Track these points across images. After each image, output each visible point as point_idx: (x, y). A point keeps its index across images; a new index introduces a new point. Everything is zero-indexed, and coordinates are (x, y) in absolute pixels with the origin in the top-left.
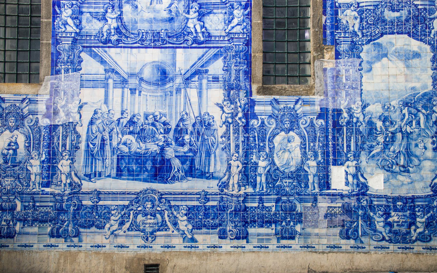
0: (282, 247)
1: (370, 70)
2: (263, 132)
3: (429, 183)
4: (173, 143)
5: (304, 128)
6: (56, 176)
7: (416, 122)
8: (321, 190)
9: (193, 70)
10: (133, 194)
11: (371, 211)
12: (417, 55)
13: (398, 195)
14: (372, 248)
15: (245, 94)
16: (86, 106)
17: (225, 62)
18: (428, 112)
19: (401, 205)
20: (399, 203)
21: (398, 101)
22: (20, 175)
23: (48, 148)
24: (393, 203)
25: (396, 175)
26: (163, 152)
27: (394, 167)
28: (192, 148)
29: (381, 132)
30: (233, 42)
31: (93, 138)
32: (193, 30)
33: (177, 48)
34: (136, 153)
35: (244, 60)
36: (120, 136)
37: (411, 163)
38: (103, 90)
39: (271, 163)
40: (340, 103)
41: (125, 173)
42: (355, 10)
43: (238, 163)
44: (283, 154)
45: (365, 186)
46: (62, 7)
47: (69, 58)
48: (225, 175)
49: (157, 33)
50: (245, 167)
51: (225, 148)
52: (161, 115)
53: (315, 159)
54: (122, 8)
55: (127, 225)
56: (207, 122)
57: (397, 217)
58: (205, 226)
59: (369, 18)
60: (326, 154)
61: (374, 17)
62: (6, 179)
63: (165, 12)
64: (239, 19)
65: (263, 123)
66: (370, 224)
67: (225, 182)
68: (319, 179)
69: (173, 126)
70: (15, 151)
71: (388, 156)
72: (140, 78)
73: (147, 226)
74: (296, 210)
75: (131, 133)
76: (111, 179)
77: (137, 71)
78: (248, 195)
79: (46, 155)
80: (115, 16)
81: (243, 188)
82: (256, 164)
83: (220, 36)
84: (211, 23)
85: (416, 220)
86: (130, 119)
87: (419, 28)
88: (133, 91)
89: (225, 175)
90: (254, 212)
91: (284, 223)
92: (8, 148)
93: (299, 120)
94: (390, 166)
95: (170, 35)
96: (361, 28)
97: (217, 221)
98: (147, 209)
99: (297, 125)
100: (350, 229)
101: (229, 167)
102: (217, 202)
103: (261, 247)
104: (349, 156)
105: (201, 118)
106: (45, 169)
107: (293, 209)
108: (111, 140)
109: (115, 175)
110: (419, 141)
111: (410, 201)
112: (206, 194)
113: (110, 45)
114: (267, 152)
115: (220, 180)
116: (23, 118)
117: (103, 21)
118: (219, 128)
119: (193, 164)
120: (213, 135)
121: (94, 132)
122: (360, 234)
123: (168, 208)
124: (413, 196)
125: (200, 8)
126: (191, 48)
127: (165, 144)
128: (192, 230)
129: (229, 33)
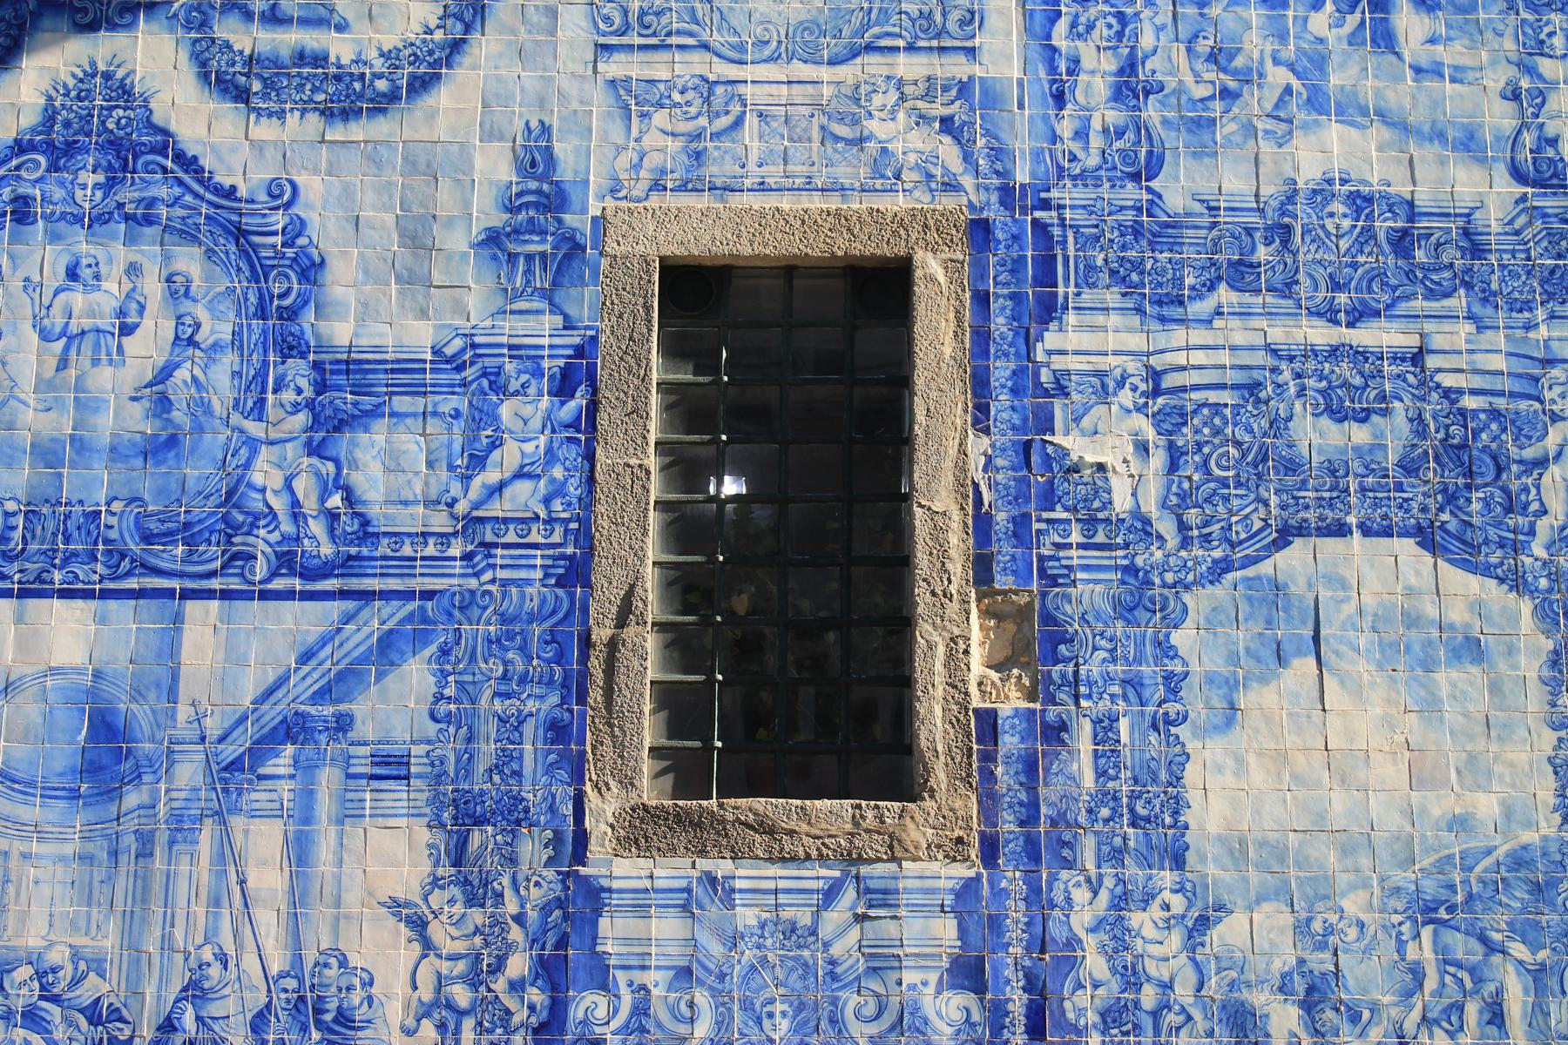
7: (1481, 1012)
9: (273, 713)
15: (550, 851)
18: (1542, 955)
30: (493, 566)
32: (279, 504)
33: (187, 595)
35: (549, 661)
40: (1068, 900)
49: (86, 515)
52: (82, 966)
56: (332, 1005)
59: (1216, 447)
61: (1238, 444)
63: (137, 409)
64: (529, 448)
65: (641, 1009)
83: (424, 534)
87: (1476, 506)
95: (154, 526)
96: (1174, 500)
99: (833, 1021)
105: (301, 981)
125: (321, 387)
126: (265, 595)
129: (473, 522)
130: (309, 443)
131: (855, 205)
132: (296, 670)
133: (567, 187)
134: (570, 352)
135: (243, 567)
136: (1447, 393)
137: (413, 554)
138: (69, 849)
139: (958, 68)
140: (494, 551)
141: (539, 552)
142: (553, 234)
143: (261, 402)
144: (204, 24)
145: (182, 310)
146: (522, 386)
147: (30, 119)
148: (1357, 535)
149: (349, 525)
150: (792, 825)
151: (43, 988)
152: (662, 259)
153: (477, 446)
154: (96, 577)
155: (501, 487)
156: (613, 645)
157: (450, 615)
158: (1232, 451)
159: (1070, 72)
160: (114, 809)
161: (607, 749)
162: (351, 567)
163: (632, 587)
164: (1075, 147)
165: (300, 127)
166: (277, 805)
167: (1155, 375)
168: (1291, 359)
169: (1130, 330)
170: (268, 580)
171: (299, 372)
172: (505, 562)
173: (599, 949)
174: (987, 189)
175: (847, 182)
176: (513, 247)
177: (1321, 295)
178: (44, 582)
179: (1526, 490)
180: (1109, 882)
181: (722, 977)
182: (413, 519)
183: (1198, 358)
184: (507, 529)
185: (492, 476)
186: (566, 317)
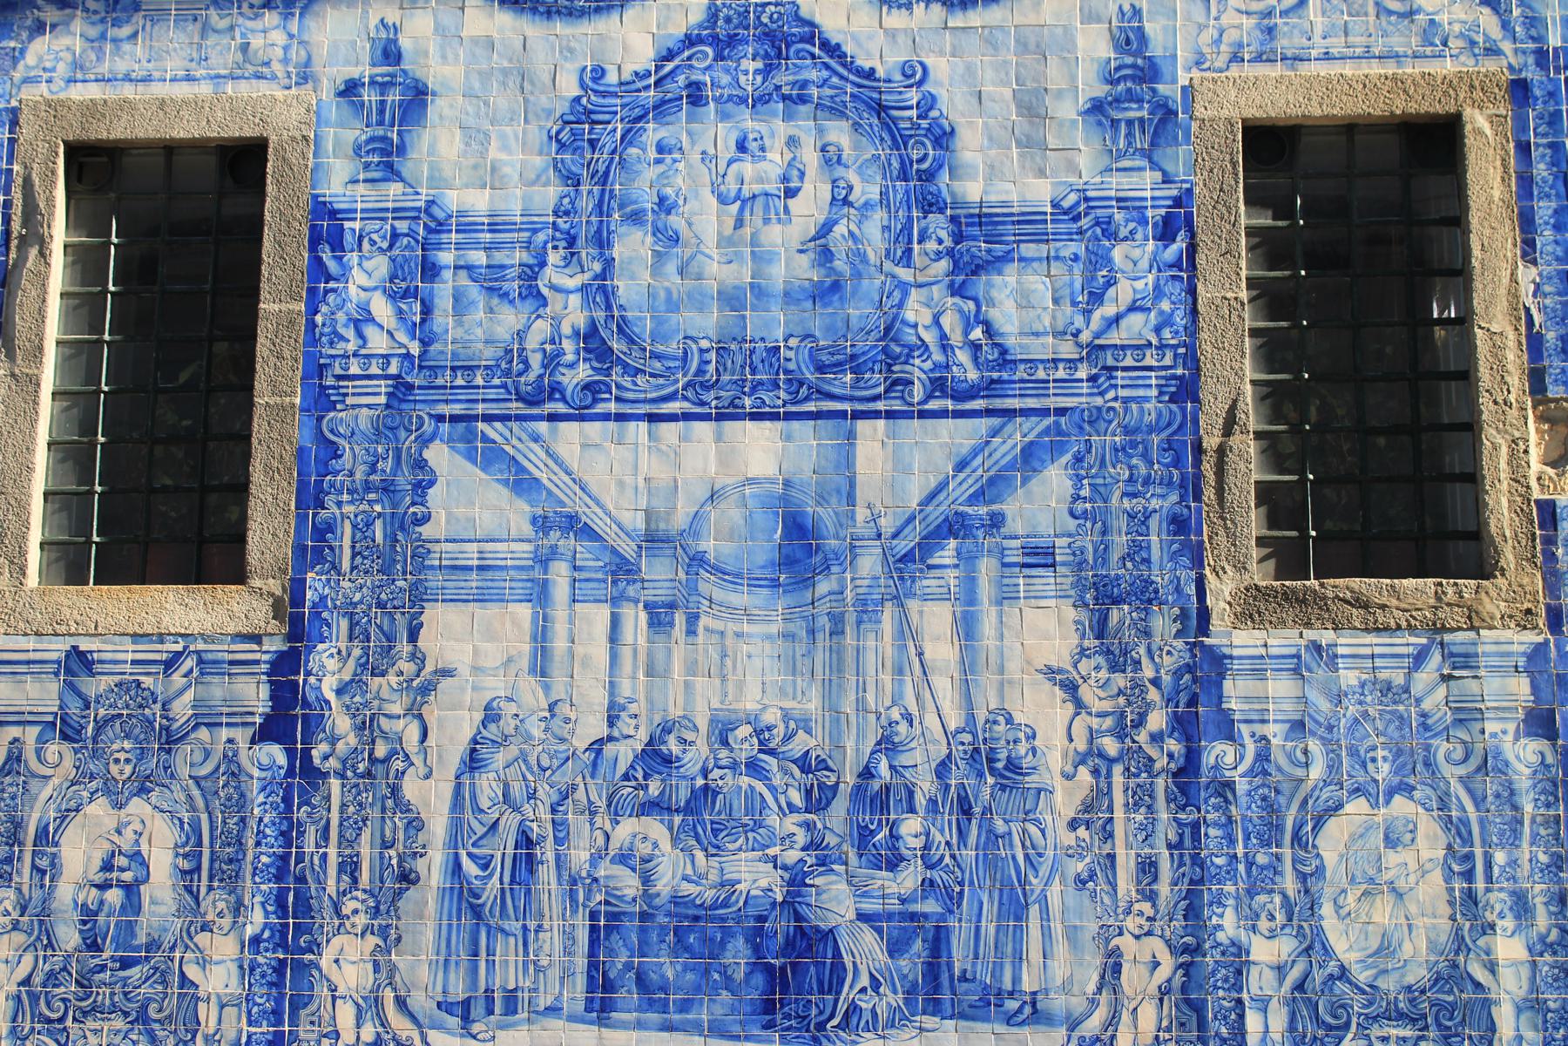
2: (1264, 799)
5: (1465, 781)
6: (313, 1007)
9: (936, 513)
15: (1178, 625)
16: (445, 684)
22: (153, 1006)
23: (279, 878)
26: (799, 894)
28: (936, 874)
30: (1115, 386)
31: (480, 830)
32: (929, 337)
33: (857, 415)
34: (676, 900)
35: (1167, 466)
38: (524, 611)
41: (628, 994)
43: (1157, 945)
46: (347, 247)
47: (373, 469)
49: (768, 350)
50: (1187, 968)
51: (1092, 876)
52: (792, 725)
54: (610, 245)
56: (1003, 755)
62: (91, 1024)
63: (804, 260)
64: (1139, 285)
65: (1263, 756)
69: (850, 779)
70: (131, 890)
72: (692, 552)
77: (680, 520)
79: (267, 914)
82: (1238, 950)
83: (1054, 361)
86: (649, 743)
88: (659, 617)
89: (1093, 1003)
92: (99, 878)
95: (825, 358)
99: (1427, 764)
101: (1113, 968)
105: (975, 735)
106: (263, 976)
109: (581, 1006)
113: (561, 408)
114: (1291, 893)
115: (1072, 1029)
116: (170, 739)
117: (529, 301)
119: (944, 954)
120: (1028, 815)
121: (484, 803)
125: (958, 238)
126: (923, 415)
127: (810, 861)
129: (1095, 349)
130: (951, 285)
131: (1410, 69)
132: (954, 477)
133: (1158, 61)
134: (1169, 203)
135: (903, 391)
137: (1046, 377)
138: (773, 629)
140: (1115, 374)
141: (1153, 374)
142: (1149, 102)
143: (908, 252)
145: (836, 175)
146: (1131, 232)
149: (990, 354)
150: (1384, 600)
151: (760, 743)
152: (1244, 121)
153: (1095, 284)
154: (780, 402)
155: (1117, 319)
156: (1221, 451)
157: (1081, 428)
160: (809, 595)
161: (1221, 538)
162: (994, 389)
163: (1235, 402)
166: (946, 590)
170: (925, 402)
171: (938, 225)
172: (1125, 382)
173: (1224, 706)
174: (1524, 52)
175: (1400, 50)
178: (736, 407)
181: (1330, 728)
182: (1044, 347)
184: (1125, 355)
185: (1109, 310)
186: (1165, 173)
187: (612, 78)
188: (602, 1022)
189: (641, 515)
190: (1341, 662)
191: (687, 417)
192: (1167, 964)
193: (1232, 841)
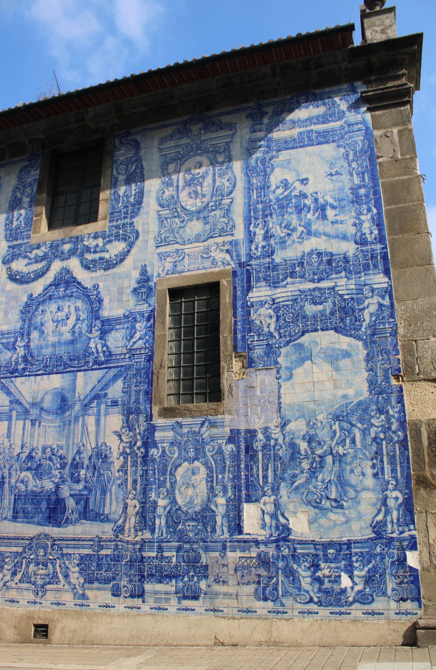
0: (183, 609)
1: (291, 377)
2: (163, 463)
3: (369, 522)
4: (69, 480)
5: (212, 456)
8: (231, 536)
9: (92, 395)
10: (26, 539)
11: (294, 563)
12: (347, 354)
13: (329, 540)
14: (296, 612)
17: (125, 383)
18: (365, 426)
19: (333, 554)
20: (331, 551)
21: (325, 414)
24: (323, 551)
25: (327, 513)
27: (323, 502)
29: (307, 457)
32: (94, 350)
34: (32, 491)
36: (19, 473)
37: (345, 495)
38: (6, 423)
39: (172, 502)
40: (254, 422)
41: (21, 515)
42: (270, 308)
43: (136, 502)
44: (186, 489)
45: (287, 529)
48: (121, 516)
50: (142, 507)
51: (122, 484)
53: (224, 495)
55: (19, 576)
56: (104, 454)
57: (329, 570)
58: (97, 579)
60: (237, 488)
61: (292, 313)
63: (69, 335)
64: (141, 333)
65: (164, 452)
66: (293, 580)
67: (121, 526)
68: (229, 520)
69: (70, 461)
71: (315, 487)
73: (39, 577)
74: (201, 561)
75: (29, 469)
76: (7, 522)
77: (39, 400)
78: (145, 542)
80: (24, 344)
81: (140, 533)
82: (155, 502)
83: (121, 354)
84: (112, 340)
85: (353, 573)
87: (348, 321)
89: (121, 516)
90: (151, 563)
91: (186, 579)
93: (205, 446)
94: (318, 500)
95: (72, 358)
96: (278, 328)
97: (110, 574)
98: (39, 557)
99: (203, 452)
100: (268, 587)
101: (126, 507)
102: (111, 550)
103: (160, 609)
104: (266, 489)
105: (98, 449)
107: (197, 559)
108: (10, 478)
109: (11, 517)
110: (355, 465)
111: (345, 547)
112: (100, 540)
113: (17, 374)
114: (168, 487)
118: (116, 461)
120: (109, 469)
122: (280, 593)
123: (60, 556)
124: (349, 540)
125: (102, 325)
126: (92, 370)
128: (84, 584)
136: (341, 296)
139: (230, 238)
143: (91, 330)
144: (83, 255)
147: (52, 279)
148: (320, 331)
150: (195, 409)
158: (291, 315)
159: (254, 235)
164: (255, 252)
165: (100, 273)
167: (274, 300)
168: (304, 292)
169: (267, 290)
171: (98, 323)
176: (138, 291)
177: (311, 277)
179: (360, 316)
180: (263, 417)
182: (118, 351)
183: (283, 295)
185: (134, 340)
186: (149, 304)
187: (34, 296)
188: (15, 521)
189: (31, 399)
190: (183, 426)
191: (42, 374)
192: (138, 506)
193: (155, 474)
